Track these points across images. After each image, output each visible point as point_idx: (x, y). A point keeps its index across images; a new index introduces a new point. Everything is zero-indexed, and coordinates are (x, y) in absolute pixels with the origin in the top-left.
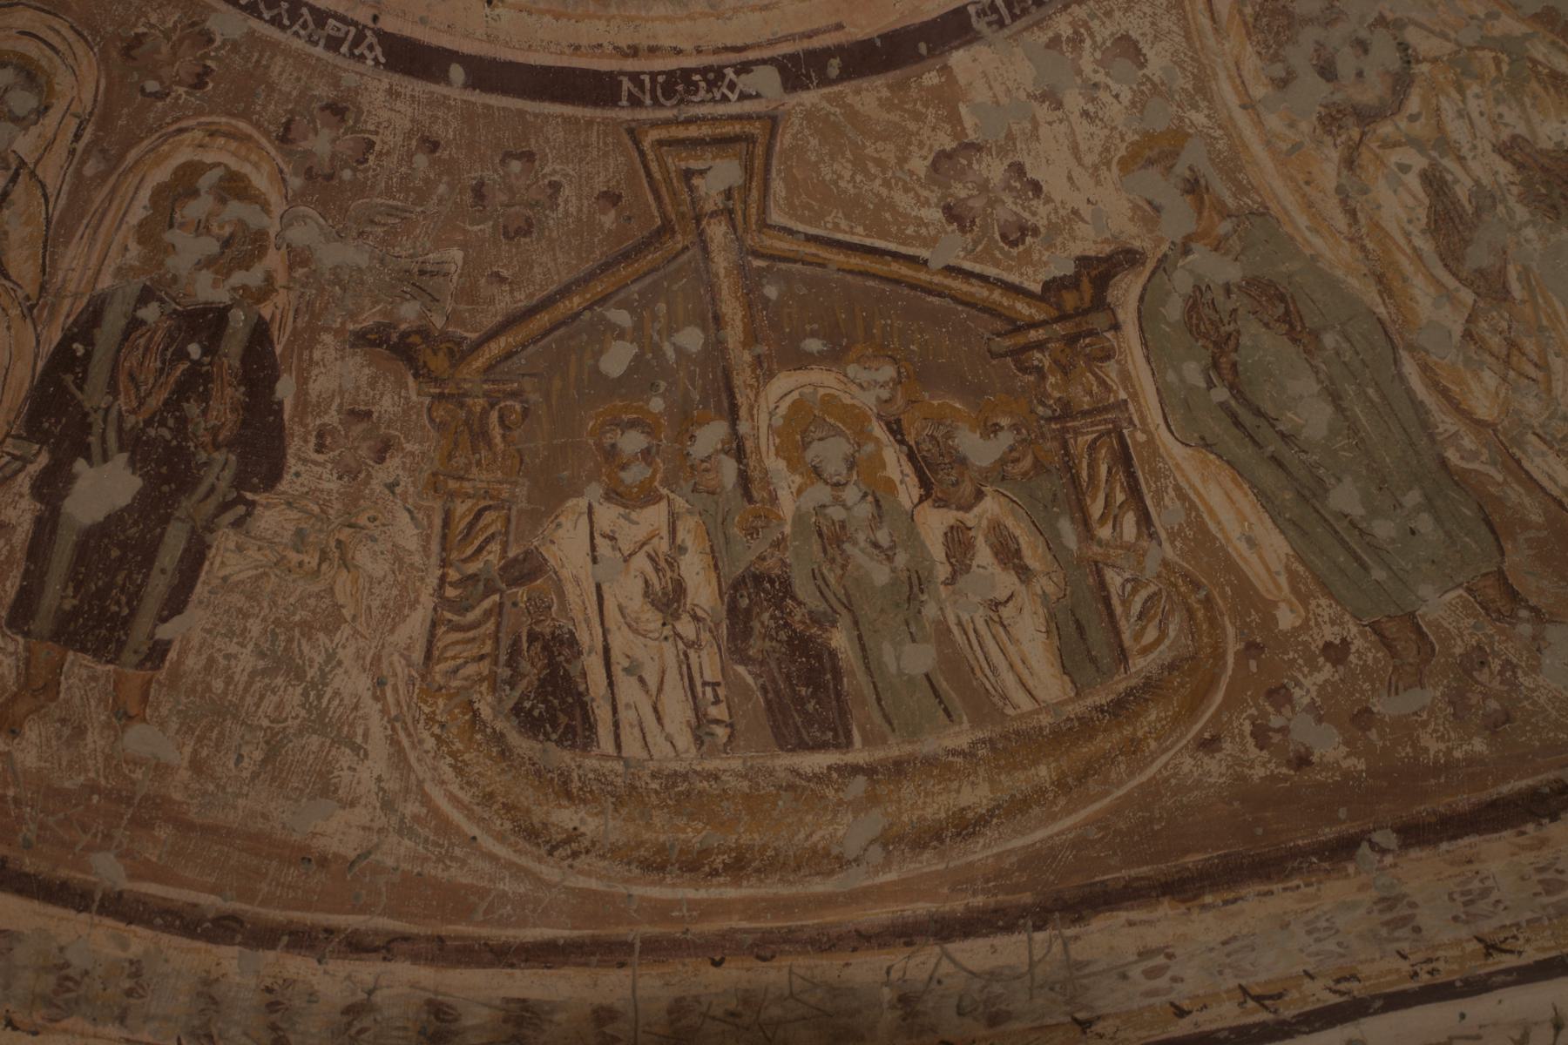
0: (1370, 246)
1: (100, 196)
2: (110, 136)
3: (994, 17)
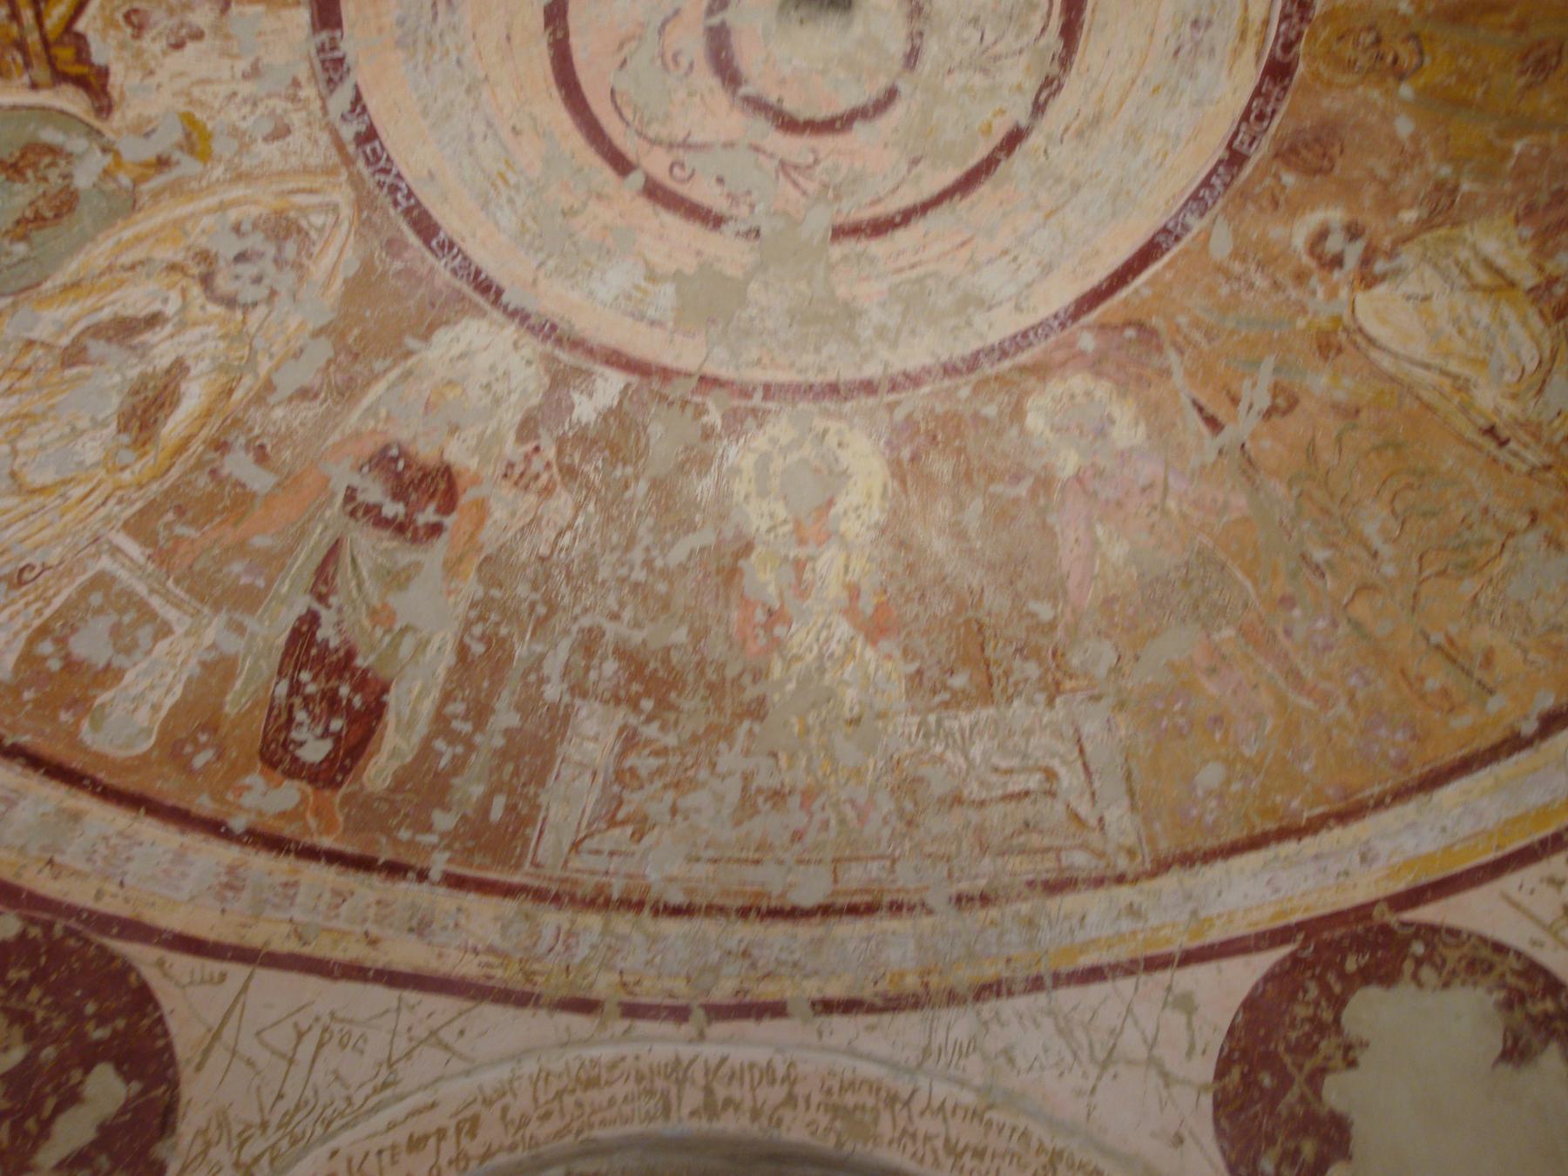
0: (103, 280)
3: (327, 46)
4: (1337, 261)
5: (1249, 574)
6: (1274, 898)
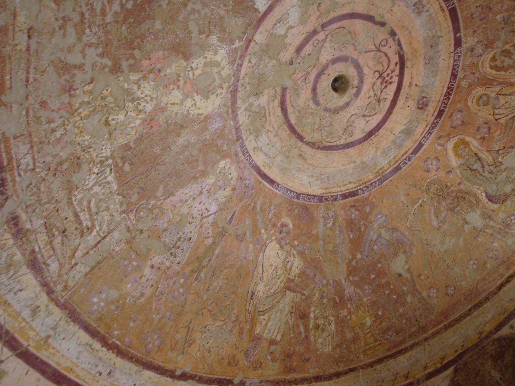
1: (501, 80)
2: (487, 82)
6: (75, 360)
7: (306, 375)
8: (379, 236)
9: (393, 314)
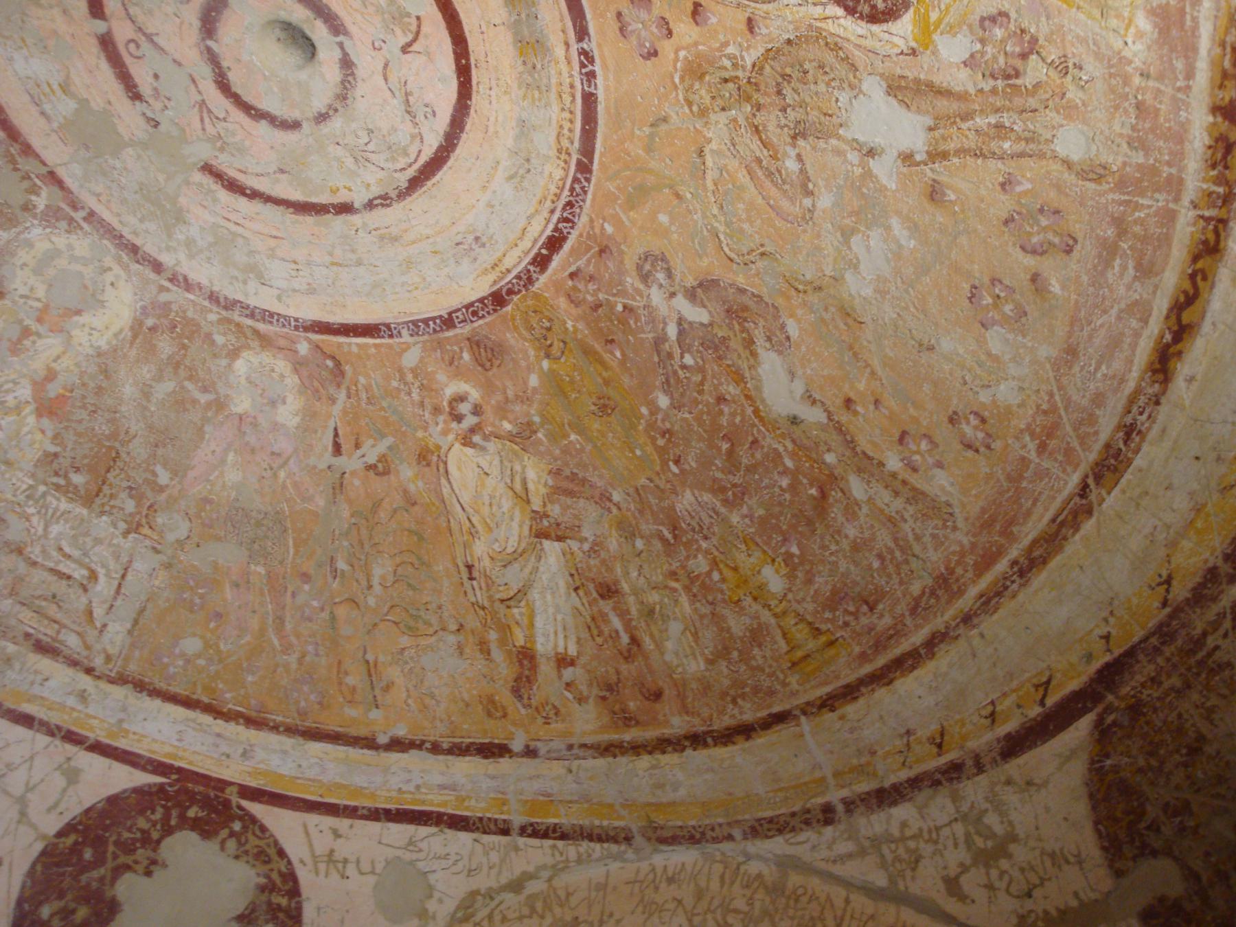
4: (459, 418)
5: (296, 546)
6: (176, 743)
7: (667, 732)
8: (680, 321)
9: (833, 548)
